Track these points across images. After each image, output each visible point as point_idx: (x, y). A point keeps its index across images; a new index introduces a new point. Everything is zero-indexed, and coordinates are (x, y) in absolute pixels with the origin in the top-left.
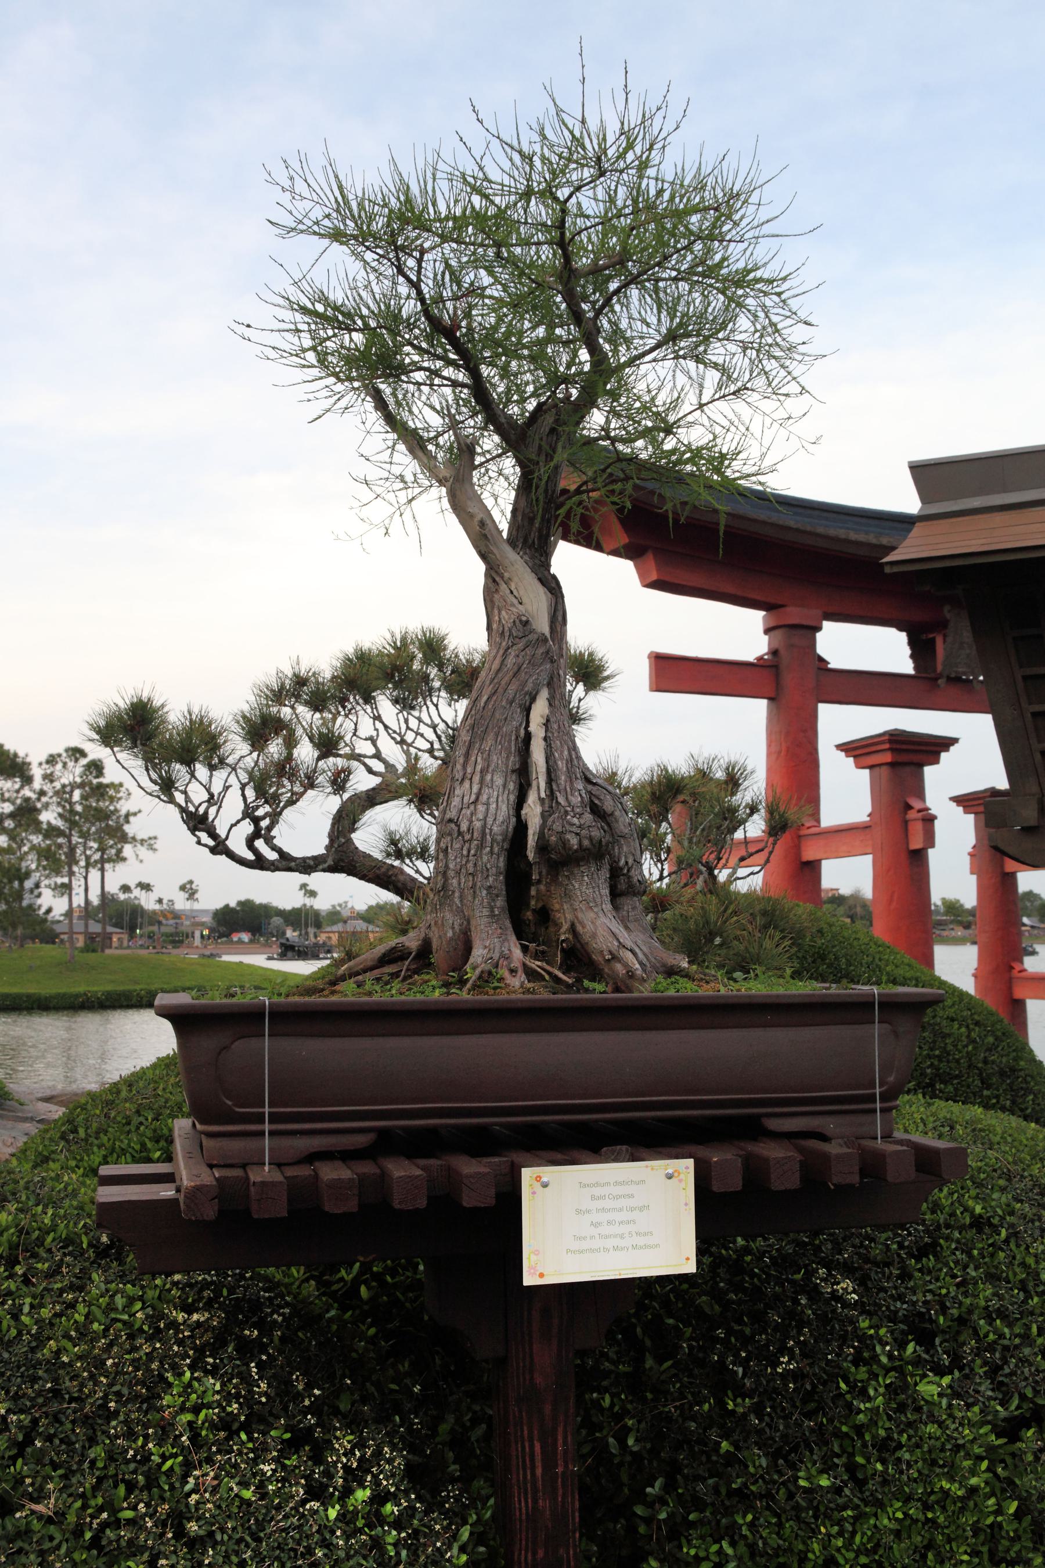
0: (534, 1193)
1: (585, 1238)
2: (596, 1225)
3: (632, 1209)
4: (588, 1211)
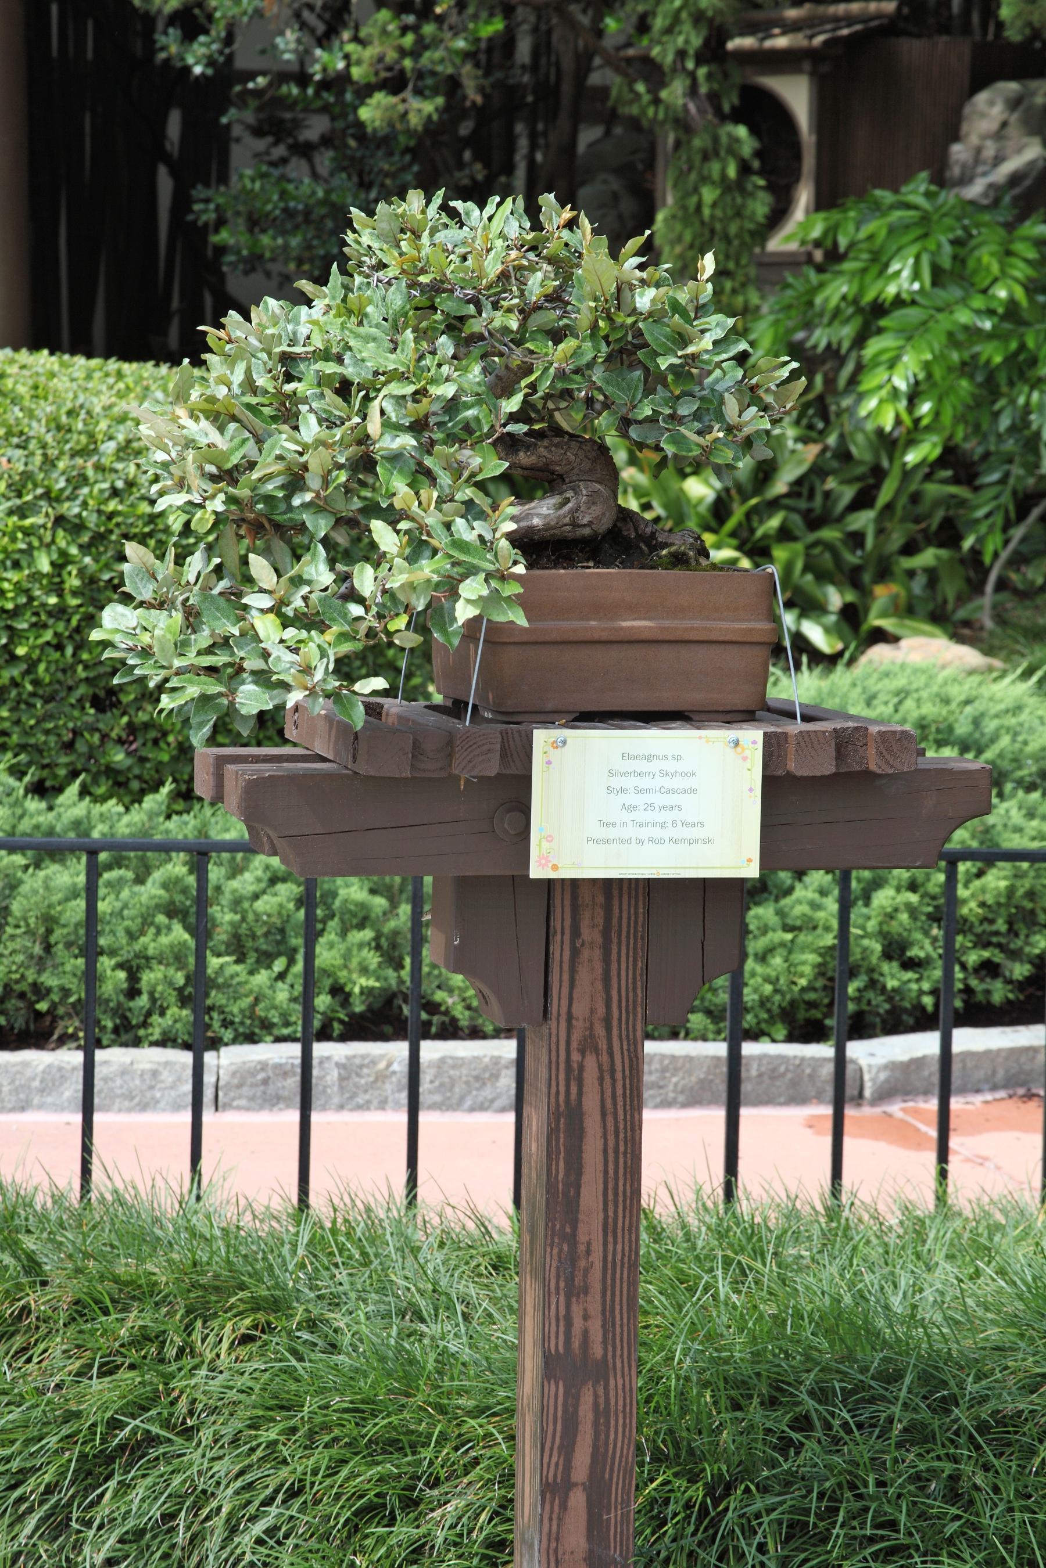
0: (549, 763)
1: (613, 824)
2: (629, 808)
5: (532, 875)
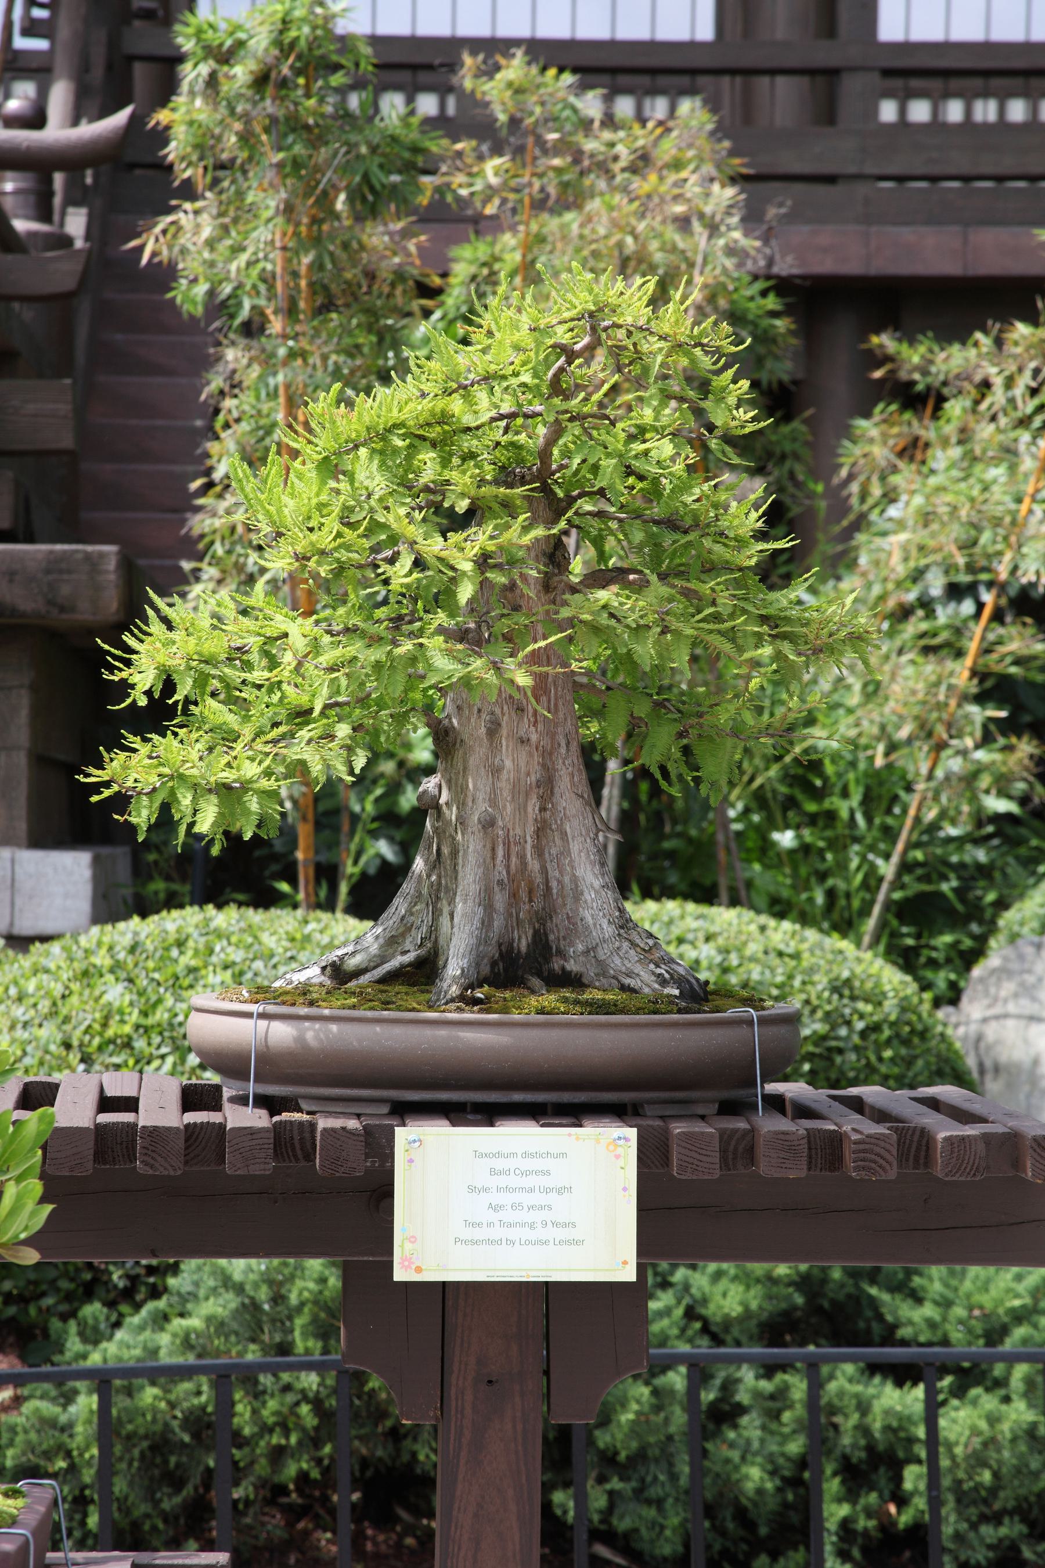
0: (411, 1161)
2: (496, 1208)
3: (547, 1190)
4: (486, 1190)
5: (397, 1277)
